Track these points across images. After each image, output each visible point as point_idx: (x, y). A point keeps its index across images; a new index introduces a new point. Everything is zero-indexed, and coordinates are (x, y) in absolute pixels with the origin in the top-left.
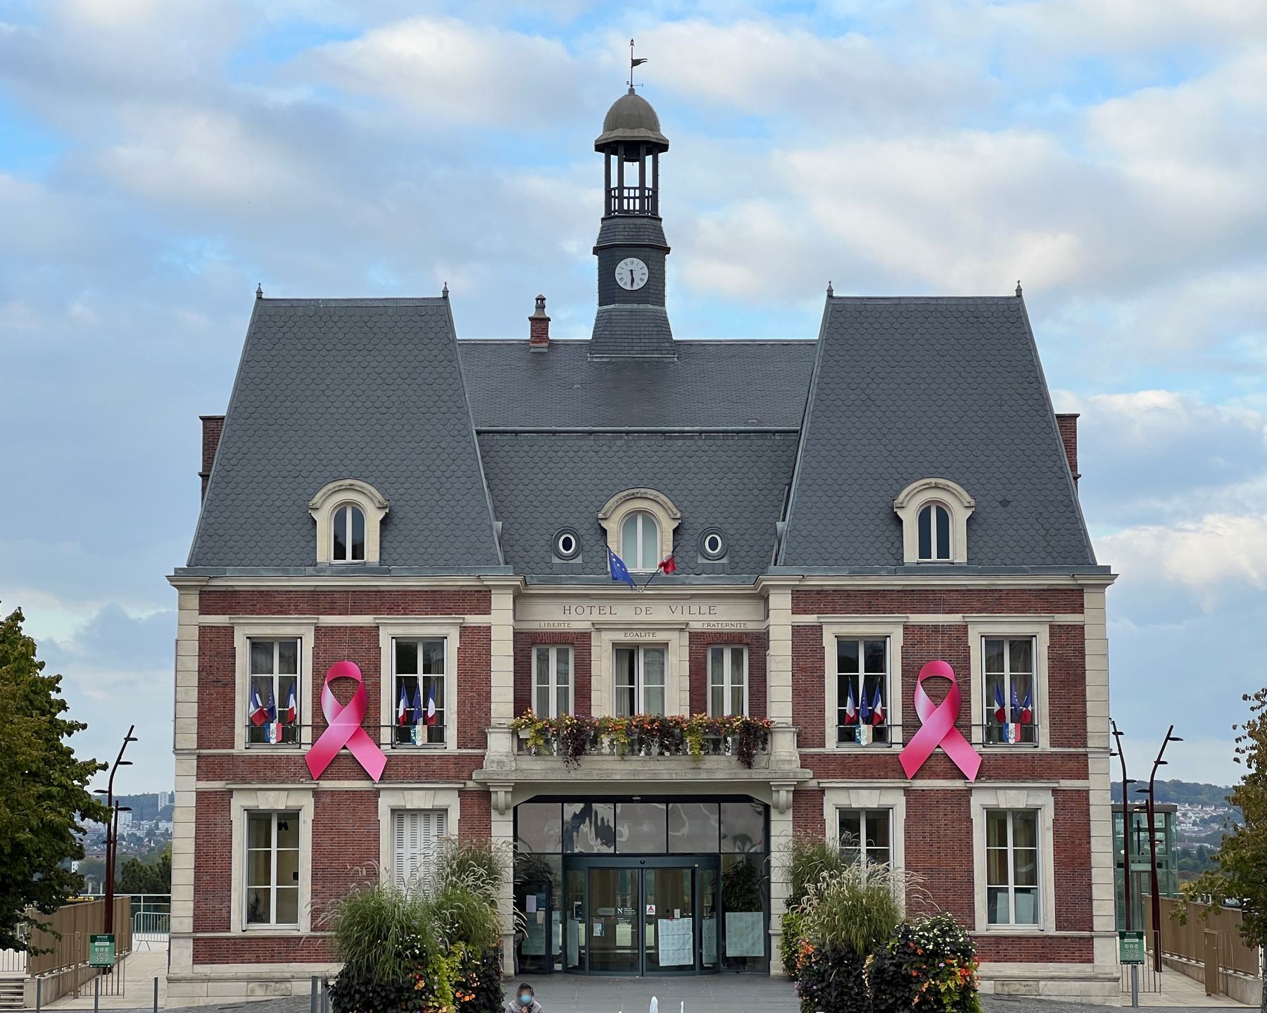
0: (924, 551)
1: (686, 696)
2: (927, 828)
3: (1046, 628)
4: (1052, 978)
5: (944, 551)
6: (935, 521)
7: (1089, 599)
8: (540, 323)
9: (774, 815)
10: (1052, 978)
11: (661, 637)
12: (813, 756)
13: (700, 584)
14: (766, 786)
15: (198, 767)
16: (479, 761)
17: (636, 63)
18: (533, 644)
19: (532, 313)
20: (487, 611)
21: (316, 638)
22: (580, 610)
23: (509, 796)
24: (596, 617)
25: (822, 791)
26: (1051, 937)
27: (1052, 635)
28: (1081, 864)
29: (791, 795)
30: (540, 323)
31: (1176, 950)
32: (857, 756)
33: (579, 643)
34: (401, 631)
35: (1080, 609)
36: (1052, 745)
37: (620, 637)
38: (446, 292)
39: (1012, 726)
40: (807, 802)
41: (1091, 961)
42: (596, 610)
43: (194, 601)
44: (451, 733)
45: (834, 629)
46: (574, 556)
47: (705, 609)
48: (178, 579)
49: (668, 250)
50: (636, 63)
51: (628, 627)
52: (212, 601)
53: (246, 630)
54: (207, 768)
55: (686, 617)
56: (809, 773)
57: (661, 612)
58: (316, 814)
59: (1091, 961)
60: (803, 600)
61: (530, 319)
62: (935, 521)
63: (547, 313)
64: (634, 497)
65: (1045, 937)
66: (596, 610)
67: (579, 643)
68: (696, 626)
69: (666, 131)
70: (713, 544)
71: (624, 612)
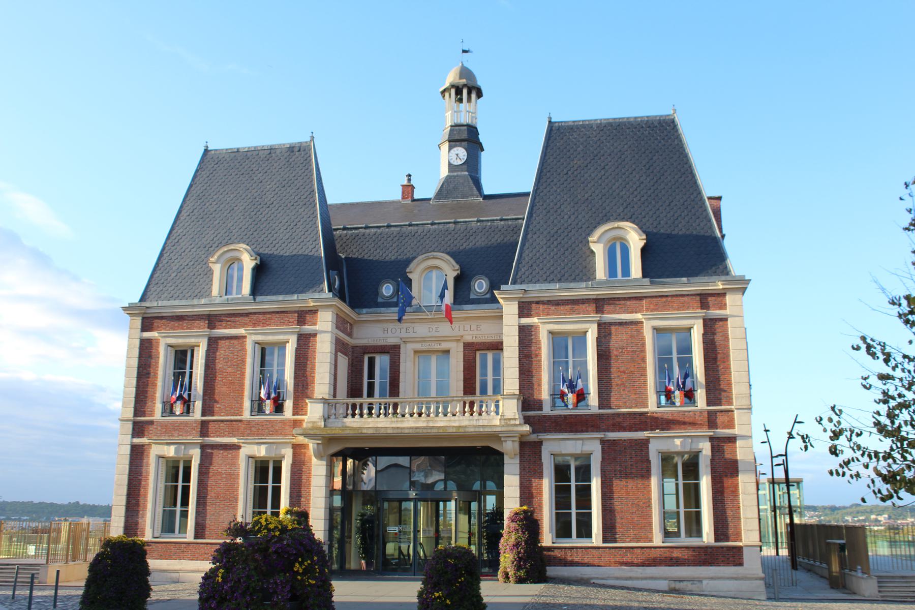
0: (612, 271)
1: (461, 384)
2: (618, 468)
3: (701, 322)
4: (712, 578)
5: (626, 271)
6: (617, 251)
7: (729, 299)
8: (408, 189)
9: (507, 460)
10: (712, 578)
11: (444, 346)
12: (534, 417)
13: (469, 311)
14: (496, 437)
15: (134, 429)
16: (301, 421)
17: (464, 51)
18: (364, 353)
19: (405, 183)
20: (315, 324)
21: (209, 345)
22: (394, 331)
23: (321, 447)
24: (404, 335)
25: (540, 444)
26: (712, 548)
27: (705, 325)
28: (733, 492)
29: (517, 445)
30: (408, 189)
31: (807, 555)
32: (565, 416)
33: (393, 351)
34: (260, 338)
35: (723, 306)
36: (708, 404)
37: (418, 346)
38: (313, 138)
39: (677, 393)
40: (530, 452)
41: (741, 564)
42: (404, 331)
43: (138, 322)
44: (288, 405)
45: (544, 326)
46: (392, 297)
47: (474, 327)
48: (130, 309)
49: (482, 150)
50: (464, 51)
51: (423, 341)
52: (147, 324)
53: (165, 341)
54: (139, 429)
55: (462, 333)
56: (527, 428)
57: (445, 329)
58: (202, 460)
59: (741, 564)
60: (525, 309)
61: (403, 186)
62: (617, 251)
63: (412, 182)
64: (428, 258)
65: (707, 547)
66: (404, 331)
67: (393, 351)
68: (469, 338)
69: (480, 83)
70: (481, 287)
71: (422, 330)
